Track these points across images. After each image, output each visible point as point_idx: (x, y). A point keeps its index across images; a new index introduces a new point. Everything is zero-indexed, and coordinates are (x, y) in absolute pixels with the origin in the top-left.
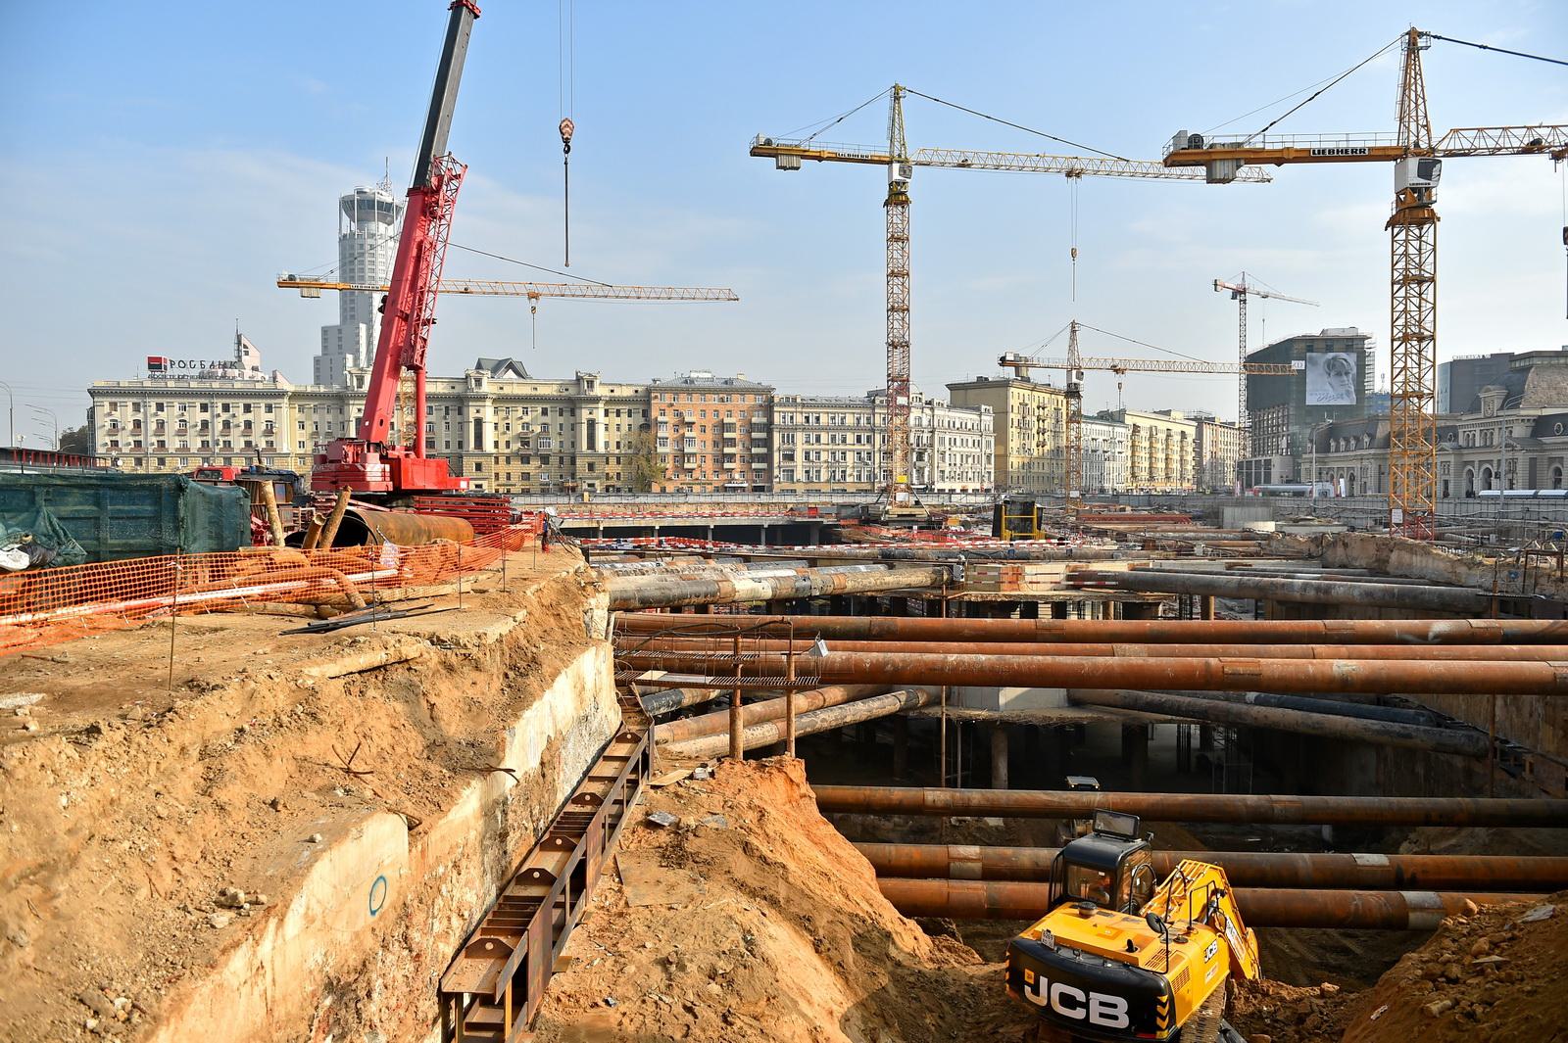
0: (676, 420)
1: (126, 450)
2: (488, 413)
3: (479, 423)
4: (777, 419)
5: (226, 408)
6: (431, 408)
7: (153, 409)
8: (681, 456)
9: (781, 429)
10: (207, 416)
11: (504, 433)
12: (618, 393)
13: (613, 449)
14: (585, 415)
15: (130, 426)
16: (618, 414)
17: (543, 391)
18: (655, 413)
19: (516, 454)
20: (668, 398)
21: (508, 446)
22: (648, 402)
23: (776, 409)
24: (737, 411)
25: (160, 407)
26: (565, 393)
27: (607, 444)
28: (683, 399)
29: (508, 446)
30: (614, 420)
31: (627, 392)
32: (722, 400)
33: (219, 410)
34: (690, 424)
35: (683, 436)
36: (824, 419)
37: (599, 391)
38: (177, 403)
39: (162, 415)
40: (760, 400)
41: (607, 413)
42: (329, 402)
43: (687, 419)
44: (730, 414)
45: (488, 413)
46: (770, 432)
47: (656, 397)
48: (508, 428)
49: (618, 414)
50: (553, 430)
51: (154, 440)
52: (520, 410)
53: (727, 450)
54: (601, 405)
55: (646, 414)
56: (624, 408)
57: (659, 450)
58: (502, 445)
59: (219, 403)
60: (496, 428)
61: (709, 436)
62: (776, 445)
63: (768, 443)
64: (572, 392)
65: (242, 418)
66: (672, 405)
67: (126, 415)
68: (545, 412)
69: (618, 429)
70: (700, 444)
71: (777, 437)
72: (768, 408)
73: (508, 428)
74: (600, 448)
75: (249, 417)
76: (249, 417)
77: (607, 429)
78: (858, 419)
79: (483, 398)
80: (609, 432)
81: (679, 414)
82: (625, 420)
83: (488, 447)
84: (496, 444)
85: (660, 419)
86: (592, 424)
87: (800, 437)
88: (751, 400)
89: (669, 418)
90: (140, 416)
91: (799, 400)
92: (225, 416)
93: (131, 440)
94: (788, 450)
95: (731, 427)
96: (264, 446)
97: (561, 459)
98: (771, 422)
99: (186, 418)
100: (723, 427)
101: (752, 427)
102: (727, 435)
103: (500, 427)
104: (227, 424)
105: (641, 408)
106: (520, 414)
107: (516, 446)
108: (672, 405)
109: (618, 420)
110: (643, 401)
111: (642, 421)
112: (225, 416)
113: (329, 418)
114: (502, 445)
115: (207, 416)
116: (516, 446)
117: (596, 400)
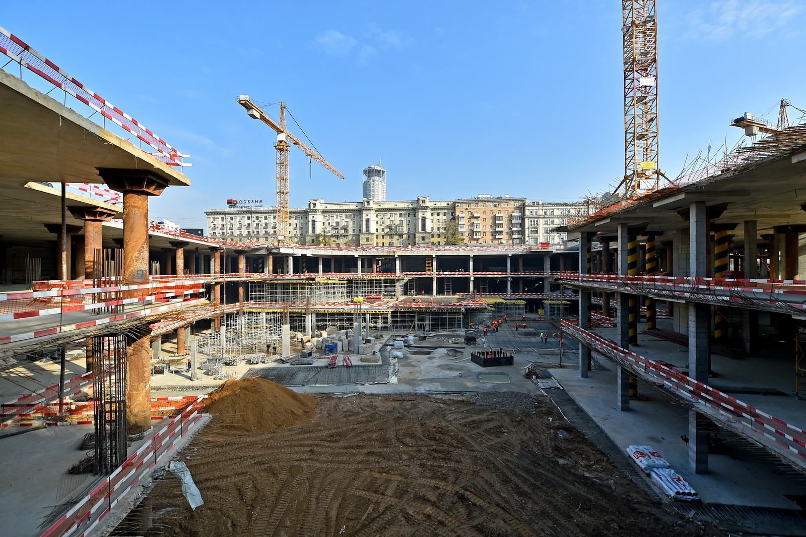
0: (470, 215)
1: (218, 236)
2: (373, 216)
3: (368, 220)
4: (527, 213)
5: (257, 218)
6: (346, 215)
7: (229, 219)
8: (472, 233)
9: (529, 218)
10: (250, 222)
11: (381, 225)
12: (438, 205)
13: (436, 230)
14: (420, 215)
15: (221, 226)
16: (438, 214)
17: (400, 206)
18: (457, 214)
19: (387, 234)
20: (465, 206)
21: (383, 231)
22: (454, 208)
23: (526, 208)
24: (504, 211)
25: (232, 219)
26: (411, 206)
27: (432, 229)
28: (473, 206)
29: (383, 231)
30: (436, 217)
31: (444, 204)
32: (495, 206)
33: (255, 219)
34: (477, 218)
35: (473, 223)
36: (556, 212)
37: (427, 204)
38: (238, 216)
39: (232, 222)
40: (517, 204)
41: (432, 214)
42: (302, 215)
43: (475, 215)
44: (500, 212)
45: (373, 216)
46: (523, 219)
47: (458, 206)
48: (383, 223)
49: (438, 214)
50: (405, 224)
51: (229, 231)
52: (389, 215)
53: (497, 229)
54: (429, 210)
55: (453, 213)
56: (442, 212)
57: (459, 230)
58: (380, 230)
59: (255, 216)
60: (377, 223)
61: (489, 221)
62: (527, 226)
63: (522, 225)
64: (415, 205)
65: (264, 221)
66: (467, 209)
67: (219, 222)
68: (401, 215)
69: (439, 222)
70: (484, 227)
71: (527, 221)
72: (522, 208)
73: (383, 223)
74: (428, 229)
75: (267, 221)
76: (267, 221)
77: (432, 222)
78: (578, 212)
79: (369, 209)
80: (433, 223)
81: (472, 213)
82: (443, 218)
83: (373, 229)
84: (377, 230)
85: (460, 216)
86: (424, 219)
87: (541, 221)
88: (512, 205)
89: (466, 215)
90: (224, 223)
91: (540, 203)
92: (257, 221)
93: (221, 232)
94: (534, 228)
95: (500, 218)
96: (273, 233)
97: (409, 237)
98: (524, 214)
99: (241, 223)
100: (495, 218)
101: (511, 218)
102: (497, 222)
103: (379, 223)
104: (257, 224)
105: (451, 211)
106: (389, 216)
107: (387, 230)
108: (467, 209)
109: (438, 218)
110: (452, 208)
111: (451, 217)
112: (257, 221)
113: (302, 221)
114: (380, 230)
115: (250, 222)
116: (387, 230)
117: (426, 208)
